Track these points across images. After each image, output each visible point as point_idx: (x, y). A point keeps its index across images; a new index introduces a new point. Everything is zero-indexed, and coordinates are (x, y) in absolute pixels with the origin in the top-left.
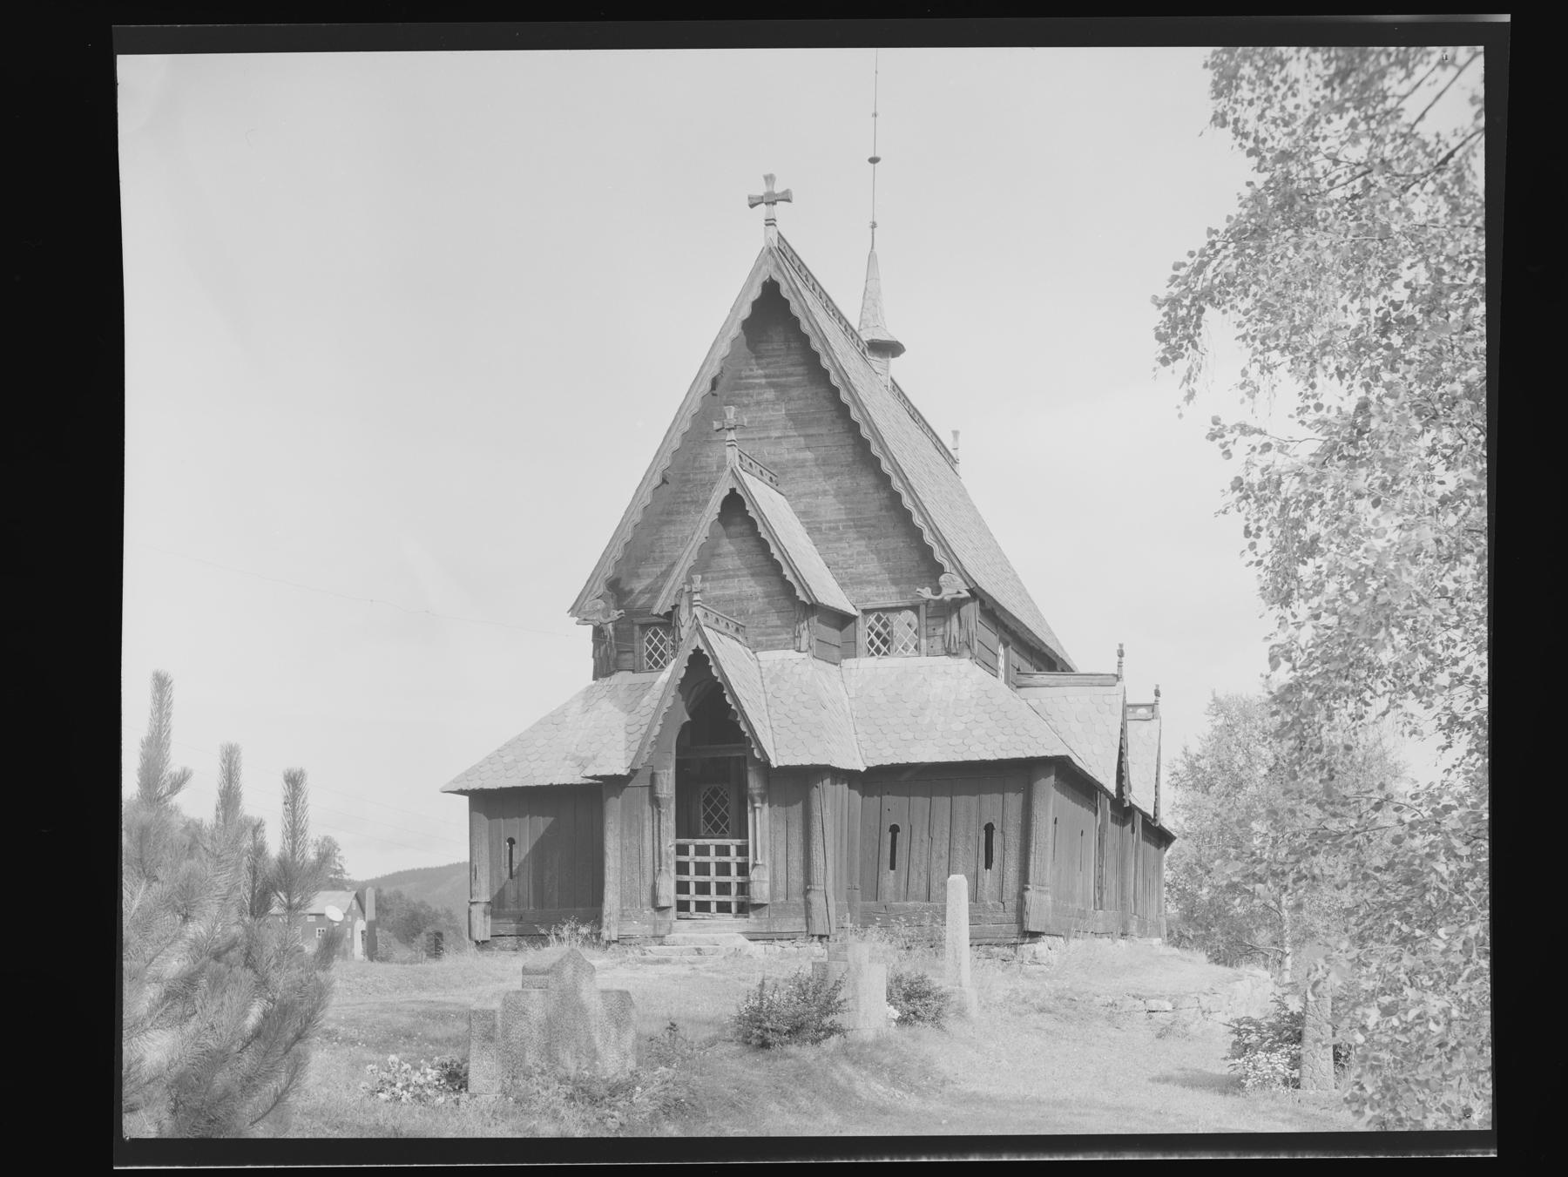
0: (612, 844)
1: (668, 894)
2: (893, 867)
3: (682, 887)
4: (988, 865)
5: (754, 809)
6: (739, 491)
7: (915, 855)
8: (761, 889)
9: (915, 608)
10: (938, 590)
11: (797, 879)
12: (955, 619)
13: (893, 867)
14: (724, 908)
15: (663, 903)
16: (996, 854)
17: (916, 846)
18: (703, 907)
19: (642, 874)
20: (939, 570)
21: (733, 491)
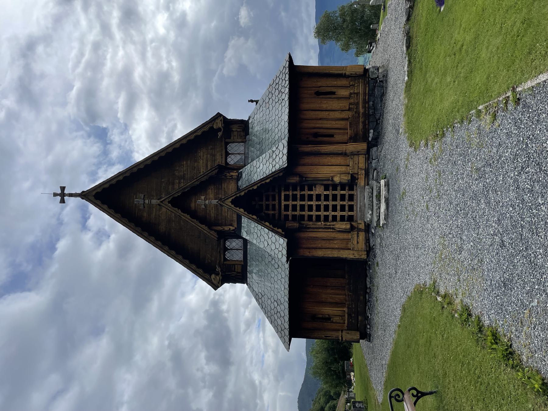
0: (320, 253)
1: (345, 225)
2: (332, 136)
3: (342, 218)
4: (334, 93)
7: (328, 126)
8: (346, 178)
9: (227, 144)
10: (219, 130)
11: (339, 160)
13: (332, 136)
14: (351, 198)
15: (348, 226)
16: (329, 89)
17: (324, 126)
18: (351, 208)
19: (334, 239)
20: (212, 128)
21: (169, 202)
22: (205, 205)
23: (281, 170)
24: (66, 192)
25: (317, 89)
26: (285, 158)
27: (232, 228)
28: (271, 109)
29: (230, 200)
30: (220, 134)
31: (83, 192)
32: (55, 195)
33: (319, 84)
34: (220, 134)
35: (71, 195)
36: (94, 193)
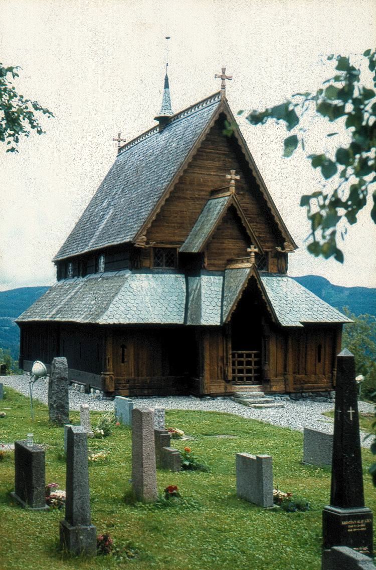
4: (319, 361)
5: (265, 341)
6: (235, 205)
11: (280, 369)
12: (283, 260)
16: (322, 357)
20: (284, 240)
22: (251, 252)
23: (276, 319)
24: (226, 80)
25: (323, 346)
26: (287, 325)
27: (206, 265)
28: (306, 302)
29: (255, 275)
30: (279, 249)
31: (227, 101)
32: (224, 70)
33: (327, 349)
34: (279, 249)
35: (223, 87)
36: (226, 113)
